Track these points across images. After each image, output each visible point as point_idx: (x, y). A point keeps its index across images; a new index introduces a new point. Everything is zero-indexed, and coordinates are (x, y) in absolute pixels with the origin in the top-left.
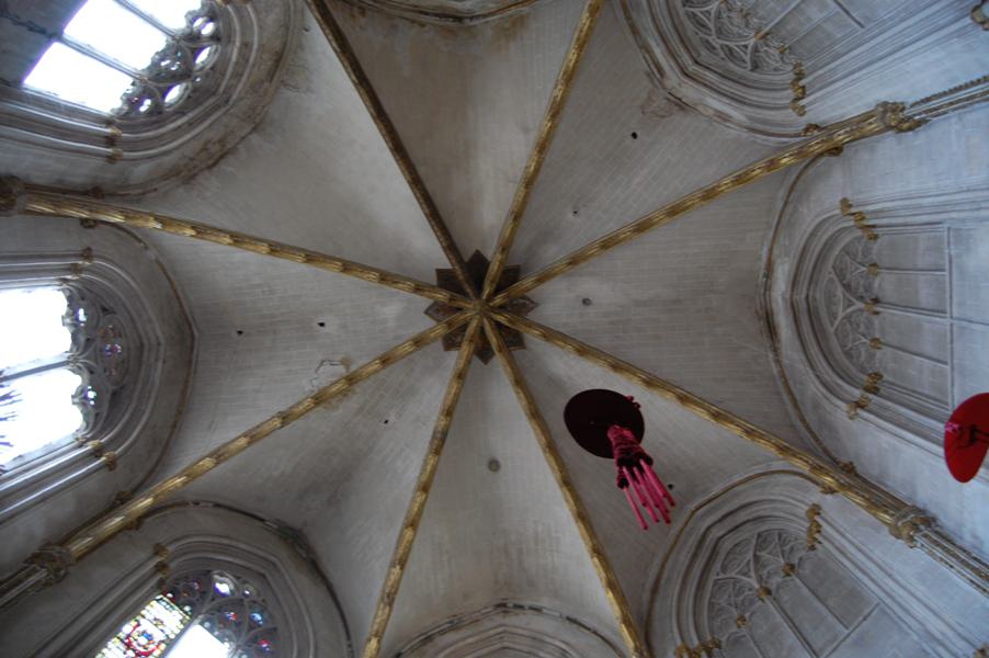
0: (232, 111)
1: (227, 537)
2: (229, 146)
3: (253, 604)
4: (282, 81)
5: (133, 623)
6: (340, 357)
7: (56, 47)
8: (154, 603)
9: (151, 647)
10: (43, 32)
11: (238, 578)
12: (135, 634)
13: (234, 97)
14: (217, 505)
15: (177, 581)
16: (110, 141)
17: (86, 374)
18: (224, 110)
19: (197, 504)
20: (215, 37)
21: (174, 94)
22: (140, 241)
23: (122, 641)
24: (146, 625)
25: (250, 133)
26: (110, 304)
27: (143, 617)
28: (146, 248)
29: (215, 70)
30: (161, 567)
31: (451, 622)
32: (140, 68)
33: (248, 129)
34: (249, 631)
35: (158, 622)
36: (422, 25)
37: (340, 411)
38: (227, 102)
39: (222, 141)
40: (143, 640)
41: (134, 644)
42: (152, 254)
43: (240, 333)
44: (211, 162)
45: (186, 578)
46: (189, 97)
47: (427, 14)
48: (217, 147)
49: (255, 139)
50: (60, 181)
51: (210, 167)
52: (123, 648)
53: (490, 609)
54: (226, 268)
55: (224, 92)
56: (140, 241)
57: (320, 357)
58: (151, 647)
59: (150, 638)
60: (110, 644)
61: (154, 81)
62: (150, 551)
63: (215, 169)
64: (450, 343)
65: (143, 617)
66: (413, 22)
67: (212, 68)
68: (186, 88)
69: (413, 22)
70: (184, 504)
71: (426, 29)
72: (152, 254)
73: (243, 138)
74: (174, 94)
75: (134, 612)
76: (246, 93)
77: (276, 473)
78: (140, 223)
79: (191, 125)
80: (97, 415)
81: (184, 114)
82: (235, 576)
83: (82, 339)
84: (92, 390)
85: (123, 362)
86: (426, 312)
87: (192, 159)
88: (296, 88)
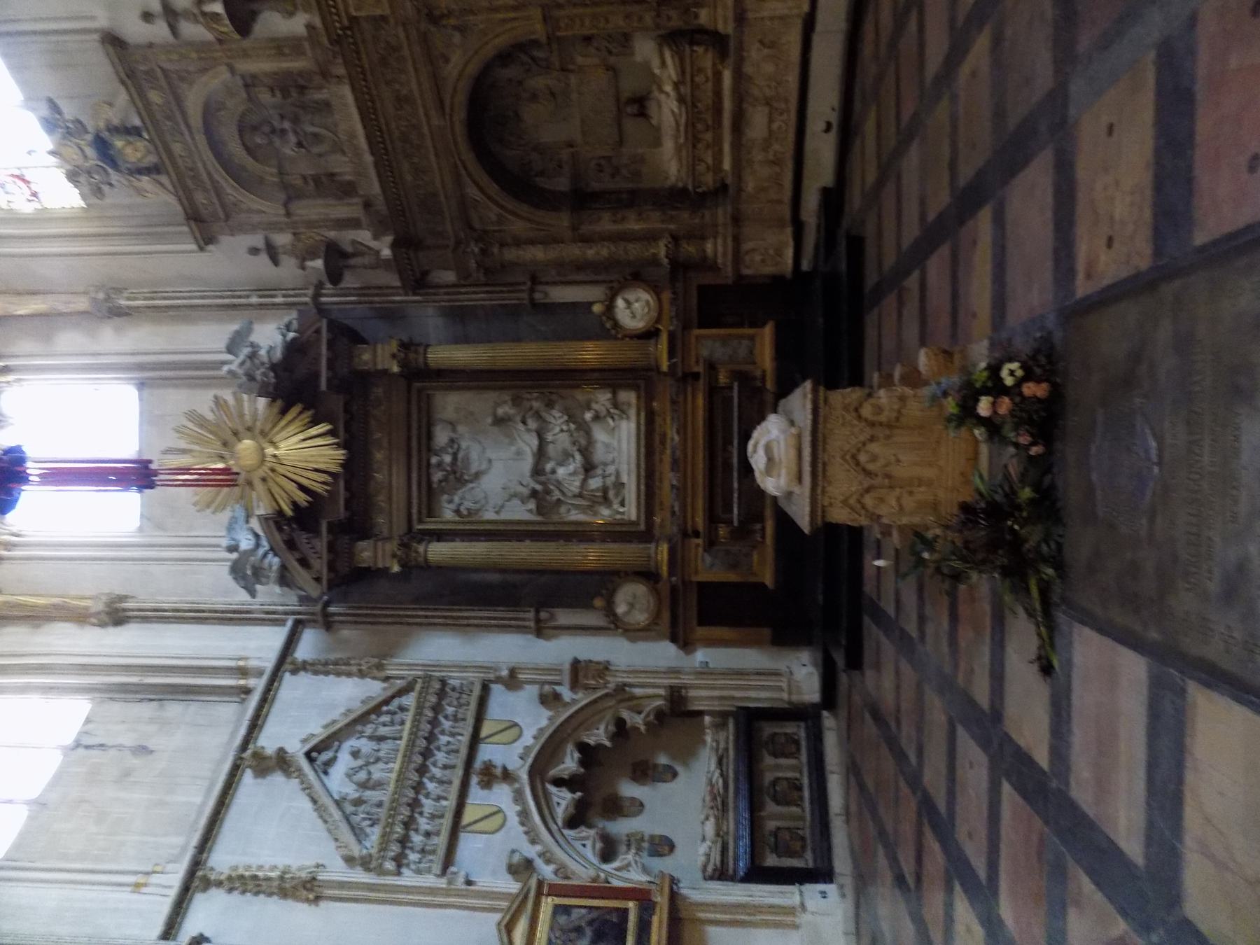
10: (87, 747)
50: (38, 626)
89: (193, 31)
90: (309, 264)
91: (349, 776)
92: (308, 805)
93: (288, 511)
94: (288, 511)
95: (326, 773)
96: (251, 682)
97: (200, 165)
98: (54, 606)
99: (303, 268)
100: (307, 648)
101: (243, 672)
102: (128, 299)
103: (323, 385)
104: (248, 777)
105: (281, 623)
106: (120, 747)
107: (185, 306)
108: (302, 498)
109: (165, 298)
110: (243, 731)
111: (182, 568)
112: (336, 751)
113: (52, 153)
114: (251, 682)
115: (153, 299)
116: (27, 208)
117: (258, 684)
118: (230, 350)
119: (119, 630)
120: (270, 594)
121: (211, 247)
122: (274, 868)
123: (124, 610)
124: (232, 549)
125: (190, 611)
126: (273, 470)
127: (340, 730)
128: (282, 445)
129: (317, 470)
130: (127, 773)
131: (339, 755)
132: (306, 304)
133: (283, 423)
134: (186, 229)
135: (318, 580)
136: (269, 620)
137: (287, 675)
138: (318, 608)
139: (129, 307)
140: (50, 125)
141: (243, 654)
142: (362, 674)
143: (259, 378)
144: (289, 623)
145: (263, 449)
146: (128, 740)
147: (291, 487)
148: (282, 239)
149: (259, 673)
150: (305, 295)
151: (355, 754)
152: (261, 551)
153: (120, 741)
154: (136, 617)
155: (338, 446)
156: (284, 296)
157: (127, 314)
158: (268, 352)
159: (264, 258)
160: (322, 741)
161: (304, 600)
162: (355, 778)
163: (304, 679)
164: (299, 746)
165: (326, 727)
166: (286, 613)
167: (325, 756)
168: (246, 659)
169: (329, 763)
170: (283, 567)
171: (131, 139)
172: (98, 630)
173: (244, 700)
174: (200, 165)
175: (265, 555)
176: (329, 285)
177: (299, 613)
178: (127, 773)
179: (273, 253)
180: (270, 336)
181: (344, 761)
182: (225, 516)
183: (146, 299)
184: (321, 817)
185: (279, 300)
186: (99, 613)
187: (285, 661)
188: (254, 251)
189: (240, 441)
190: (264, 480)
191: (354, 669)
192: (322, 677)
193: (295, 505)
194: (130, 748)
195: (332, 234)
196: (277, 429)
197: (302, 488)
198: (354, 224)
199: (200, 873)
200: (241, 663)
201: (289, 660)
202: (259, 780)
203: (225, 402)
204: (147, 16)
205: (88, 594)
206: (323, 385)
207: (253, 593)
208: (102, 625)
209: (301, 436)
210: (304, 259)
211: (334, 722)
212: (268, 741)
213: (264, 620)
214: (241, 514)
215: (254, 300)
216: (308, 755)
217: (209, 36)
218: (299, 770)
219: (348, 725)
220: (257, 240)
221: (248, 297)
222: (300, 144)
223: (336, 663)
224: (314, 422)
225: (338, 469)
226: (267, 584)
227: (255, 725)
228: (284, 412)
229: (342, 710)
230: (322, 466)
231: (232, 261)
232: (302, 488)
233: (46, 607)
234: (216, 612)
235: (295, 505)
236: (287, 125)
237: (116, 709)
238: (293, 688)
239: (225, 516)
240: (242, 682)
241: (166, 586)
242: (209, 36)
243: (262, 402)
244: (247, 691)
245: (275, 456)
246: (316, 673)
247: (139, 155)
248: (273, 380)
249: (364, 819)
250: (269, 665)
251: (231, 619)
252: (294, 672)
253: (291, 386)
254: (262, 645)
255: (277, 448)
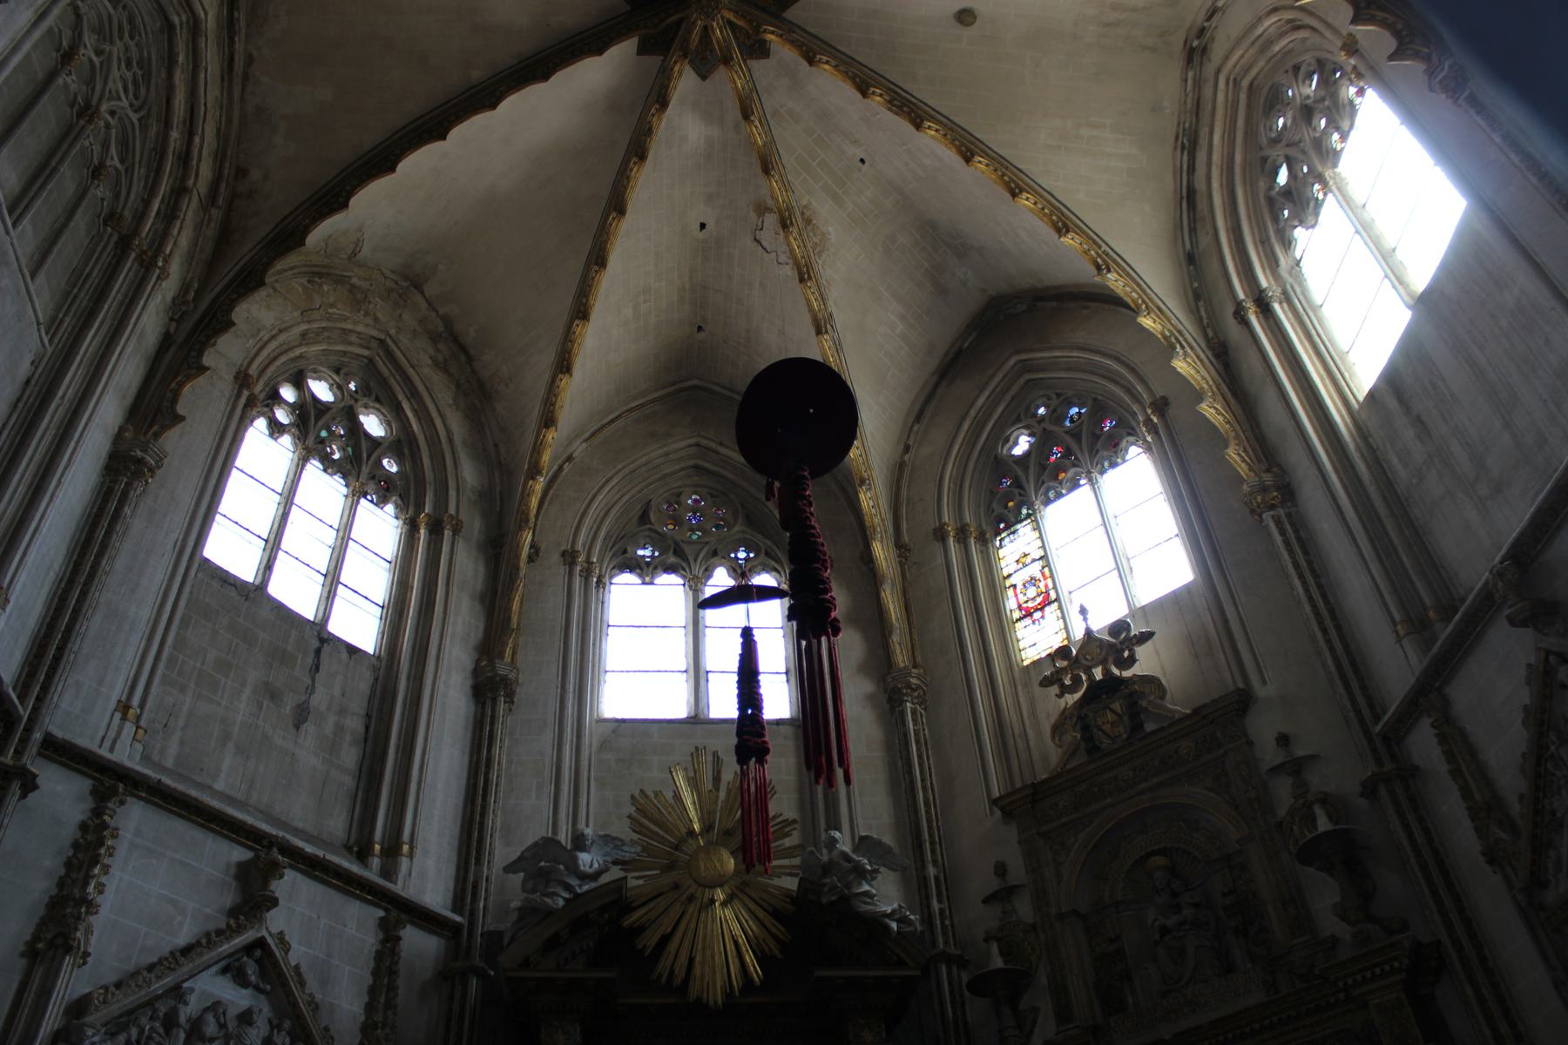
0: (392, 332)
1: (963, 419)
2: (441, 329)
3: (1057, 416)
4: (349, 258)
5: (1010, 592)
6: (753, 215)
7: (334, 627)
8: (1002, 553)
9: (1042, 585)
10: (318, 651)
11: (1018, 420)
12: (1022, 599)
13: (375, 333)
14: (918, 418)
15: (990, 510)
16: (436, 529)
17: (715, 560)
18: (393, 346)
19: (907, 449)
20: (299, 383)
21: (373, 425)
22: (560, 468)
23: (1021, 619)
24: (1017, 579)
25: (422, 293)
26: (636, 511)
27: (1009, 576)
28: (569, 459)
29: (337, 372)
30: (962, 535)
31: (1183, 147)
32: (345, 490)
33: (419, 298)
34: (1079, 441)
35: (1022, 561)
36: (250, 60)
37: (831, 229)
38: (382, 341)
39: (434, 338)
40: (1032, 592)
41: (1030, 604)
42: (579, 449)
43: (700, 329)
44: (463, 358)
45: (993, 494)
46: (377, 400)
47: (232, 59)
48: (441, 346)
49: (431, 289)
51: (470, 359)
52: (1028, 621)
53: (1190, 74)
54: (615, 337)
55: (368, 348)
56: (560, 468)
57: (749, 241)
58: (1042, 585)
59: (1033, 581)
60: (1019, 635)
61: (359, 469)
62: (938, 546)
63: (472, 352)
64: (762, 51)
65: (1009, 576)
66: (246, 77)
67: (337, 371)
68: (366, 407)
69: (246, 77)
70: (901, 466)
71: (255, 53)
72: (579, 449)
73: (430, 304)
74: (373, 425)
75: (996, 586)
76: (367, 314)
77: (900, 328)
78: (546, 457)
79: (413, 394)
80: (767, 554)
81: (399, 404)
82: (1014, 424)
83: (672, 559)
84: (736, 551)
85: (712, 496)
86: (704, 78)
87: (458, 385)
88: (358, 244)
89: (1283, 793)
90: (995, 948)
91: (217, 1004)
92: (182, 940)
93: (627, 922)
94: (627, 922)
95: (224, 971)
96: (375, 862)
97: (1109, 800)
98: (509, 619)
99: (986, 940)
100: (418, 944)
101: (392, 851)
102: (914, 712)
103: (820, 973)
104: (240, 854)
105: (457, 905)
106: (312, 689)
107: (912, 781)
108: (650, 940)
109: (920, 757)
110: (309, 849)
111: (547, 773)
112: (257, 988)
113: (1088, 632)
114: (375, 862)
115: (917, 742)
116: (1011, 604)
117: (371, 872)
118: (863, 844)
119: (469, 691)
120: (504, 889)
121: (998, 813)
122: (101, 889)
123: (494, 700)
124: (579, 842)
125: (486, 781)
126: (691, 899)
127: (289, 993)
128: (729, 913)
129: (691, 960)
130: (274, 695)
131: (249, 991)
132: (934, 943)
133: (760, 913)
134: (1018, 785)
135: (526, 963)
136: (464, 890)
137: (381, 913)
138: (477, 962)
139: (903, 714)
140: (1118, 628)
141: (418, 852)
142: (367, 1028)
143: (828, 880)
144: (458, 919)
145: (721, 886)
146: (319, 699)
147: (666, 925)
148: (1024, 909)
149: (389, 872)
150: (946, 943)
151: (246, 1018)
152: (574, 882)
153: (320, 689)
154: (483, 714)
155: (729, 994)
156: (942, 912)
157: (892, 709)
158: (866, 894)
159: (994, 884)
160: (276, 964)
161: (494, 941)
162: (210, 1018)
163: (370, 940)
164: (274, 930)
165: (297, 967)
166: (473, 914)
167: (251, 970)
168: (411, 856)
169: (241, 979)
170: (550, 913)
171: (1126, 718)
172: (470, 666)
173: (348, 848)
174: (1109, 800)
175: (568, 887)
176: (965, 977)
177: (470, 934)
178: (274, 695)
179: (1002, 896)
180: (885, 895)
181: (237, 998)
182: (621, 829)
183: (916, 734)
184: (160, 962)
185: (935, 905)
186: (494, 668)
187: (401, 911)
188: (1001, 870)
189: (732, 853)
190: (676, 886)
191: (379, 1018)
192: (372, 964)
193: (639, 930)
194: (307, 702)
195: (1043, 980)
196: (752, 906)
197: (665, 940)
198: (1063, 1014)
199: (121, 787)
200: (406, 848)
201: (404, 917)
202: (233, 870)
203: (788, 835)
204: (1283, 740)
205: (519, 657)
206: (820, 973)
207: (510, 868)
208: (476, 672)
209: (742, 940)
210: (999, 940)
211: (302, 984)
212: (291, 886)
213: (465, 879)
214: (629, 853)
215: (931, 870)
216: (261, 943)
217: (1282, 812)
218: (239, 930)
219: (295, 1005)
220: (1018, 871)
221: (935, 862)
222: (1165, 931)
223: (392, 988)
224: (762, 958)
225: (694, 991)
226: (524, 890)
227: (315, 868)
228: (776, 914)
229: (318, 997)
230: (697, 970)
231: (981, 841)
232: (665, 940)
233: (508, 610)
234: (483, 815)
235: (639, 930)
236: (1187, 912)
237: (363, 683)
238: (358, 923)
239: (621, 829)
240: (377, 847)
241: (524, 749)
242: (1282, 812)
243: (791, 884)
244: (362, 855)
245: (712, 901)
246: (379, 956)
247: (1107, 728)
248: (824, 901)
249: (142, 1031)
250: (398, 888)
251: (470, 836)
252: (383, 924)
253: (814, 921)
254: (428, 877)
255: (724, 904)
